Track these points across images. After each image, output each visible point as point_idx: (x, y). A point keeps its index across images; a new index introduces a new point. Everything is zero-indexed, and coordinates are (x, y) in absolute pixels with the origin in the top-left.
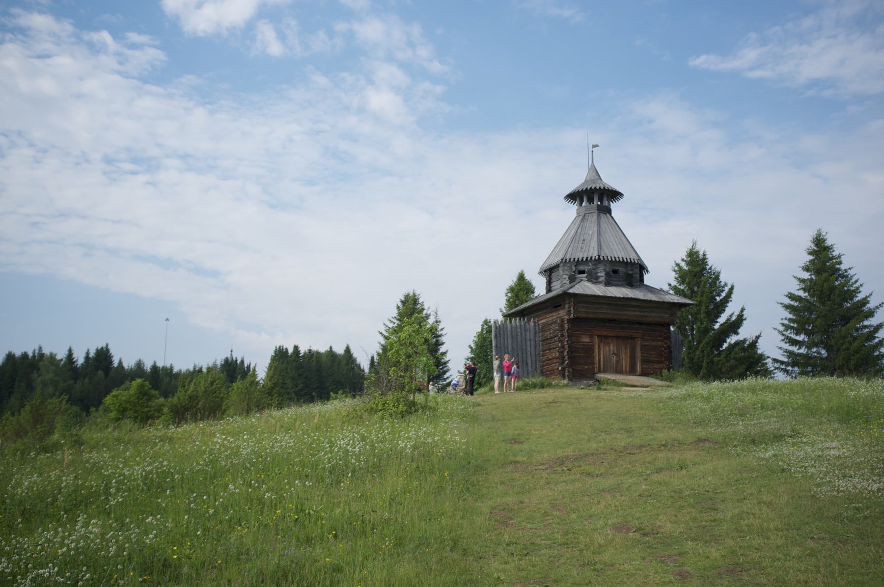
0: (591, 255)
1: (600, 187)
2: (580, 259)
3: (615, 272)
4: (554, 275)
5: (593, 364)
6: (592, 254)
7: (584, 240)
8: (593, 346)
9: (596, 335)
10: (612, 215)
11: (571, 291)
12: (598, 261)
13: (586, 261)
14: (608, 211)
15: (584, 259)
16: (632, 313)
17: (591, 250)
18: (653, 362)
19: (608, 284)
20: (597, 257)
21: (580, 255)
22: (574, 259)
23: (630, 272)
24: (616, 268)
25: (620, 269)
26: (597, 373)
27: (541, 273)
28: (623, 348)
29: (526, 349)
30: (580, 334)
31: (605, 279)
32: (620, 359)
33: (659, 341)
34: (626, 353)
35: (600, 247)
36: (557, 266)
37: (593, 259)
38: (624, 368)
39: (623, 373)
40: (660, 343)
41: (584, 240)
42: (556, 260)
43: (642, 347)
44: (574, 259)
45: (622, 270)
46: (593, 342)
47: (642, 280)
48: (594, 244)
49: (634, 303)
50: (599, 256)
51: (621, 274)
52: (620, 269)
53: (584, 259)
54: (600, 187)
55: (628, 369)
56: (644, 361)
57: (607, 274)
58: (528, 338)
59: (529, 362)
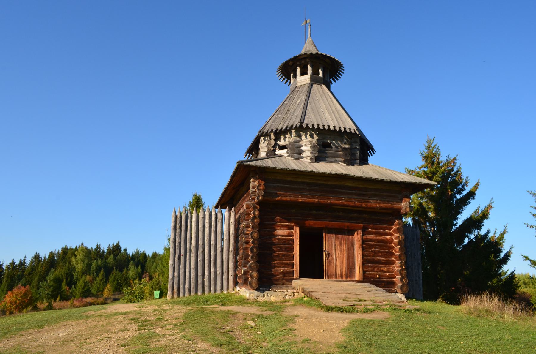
0: (292, 124)
2: (279, 129)
5: (292, 265)
6: (294, 122)
7: (289, 110)
8: (293, 240)
10: (331, 90)
17: (294, 119)
26: (296, 279)
28: (338, 243)
31: (311, 153)
34: (342, 251)
38: (338, 272)
41: (289, 110)
43: (364, 242)
46: (292, 236)
48: (299, 112)
49: (349, 184)
55: (344, 273)
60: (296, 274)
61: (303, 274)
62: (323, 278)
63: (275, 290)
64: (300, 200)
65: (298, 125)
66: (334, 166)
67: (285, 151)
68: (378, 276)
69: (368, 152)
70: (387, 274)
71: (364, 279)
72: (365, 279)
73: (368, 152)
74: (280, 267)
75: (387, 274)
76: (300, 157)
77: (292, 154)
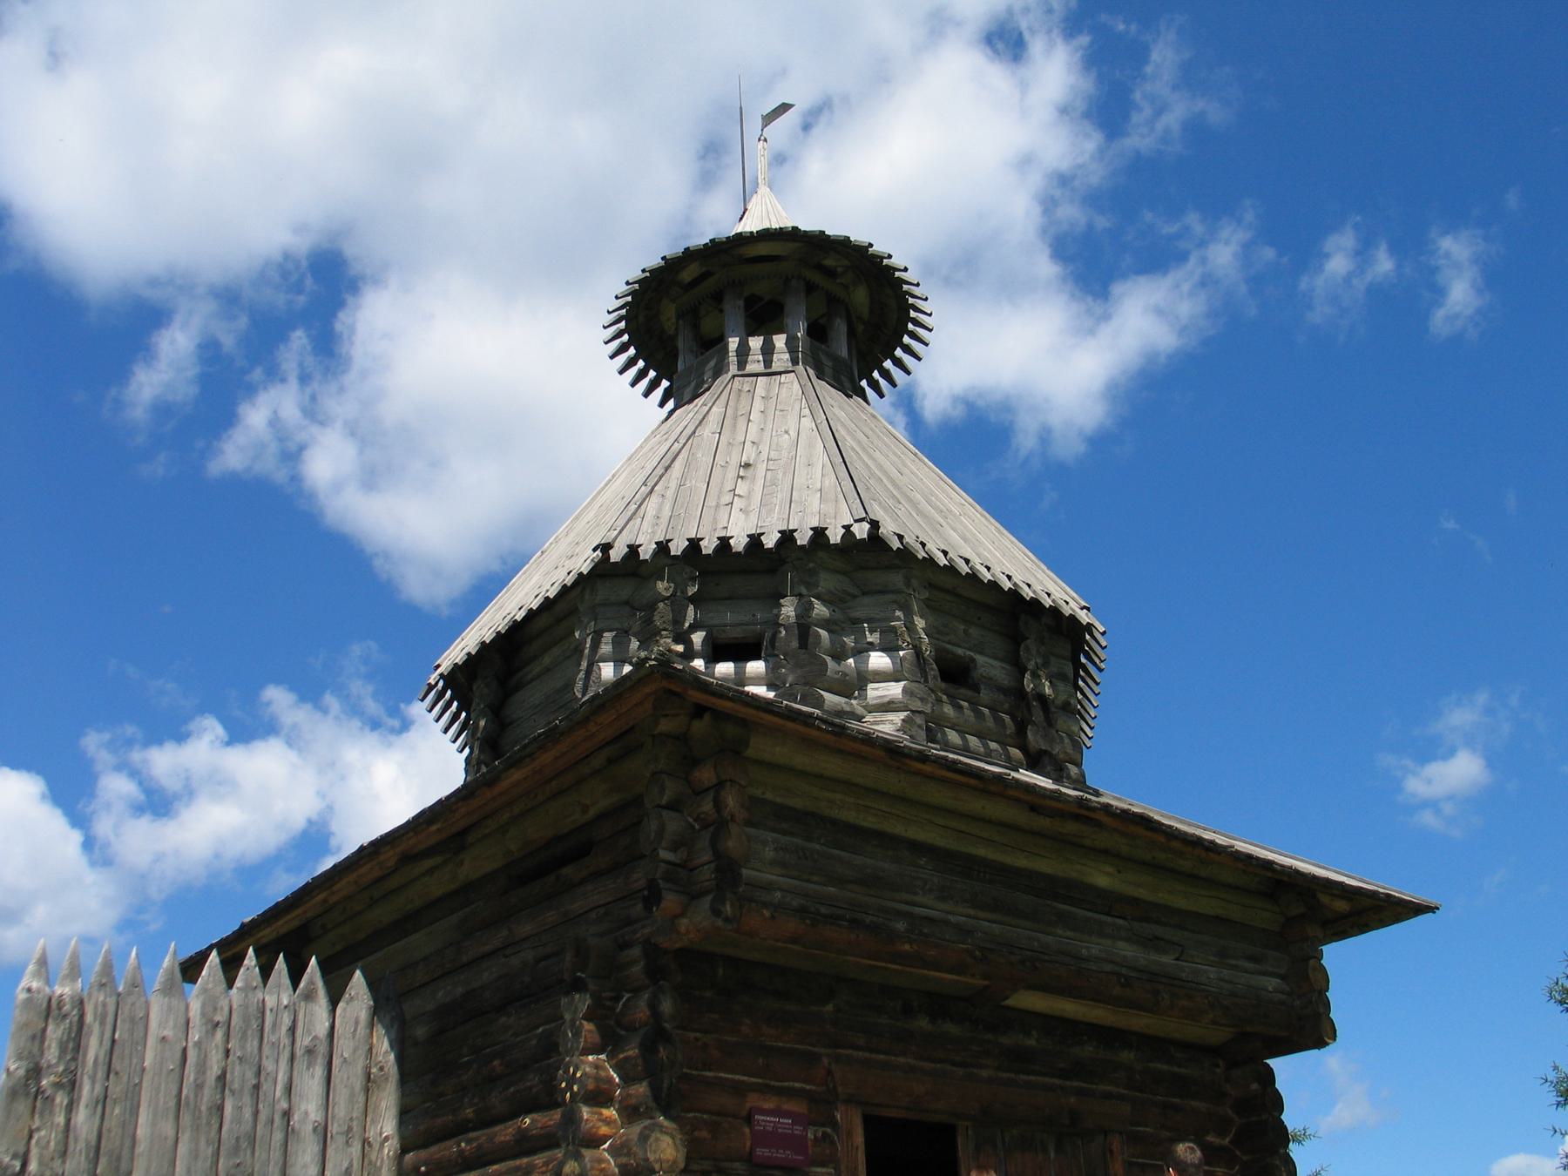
25: (980, 659)
30: (740, 1090)
52: (980, 659)
58: (309, 1108)
65: (861, 531)
77: (806, 684)
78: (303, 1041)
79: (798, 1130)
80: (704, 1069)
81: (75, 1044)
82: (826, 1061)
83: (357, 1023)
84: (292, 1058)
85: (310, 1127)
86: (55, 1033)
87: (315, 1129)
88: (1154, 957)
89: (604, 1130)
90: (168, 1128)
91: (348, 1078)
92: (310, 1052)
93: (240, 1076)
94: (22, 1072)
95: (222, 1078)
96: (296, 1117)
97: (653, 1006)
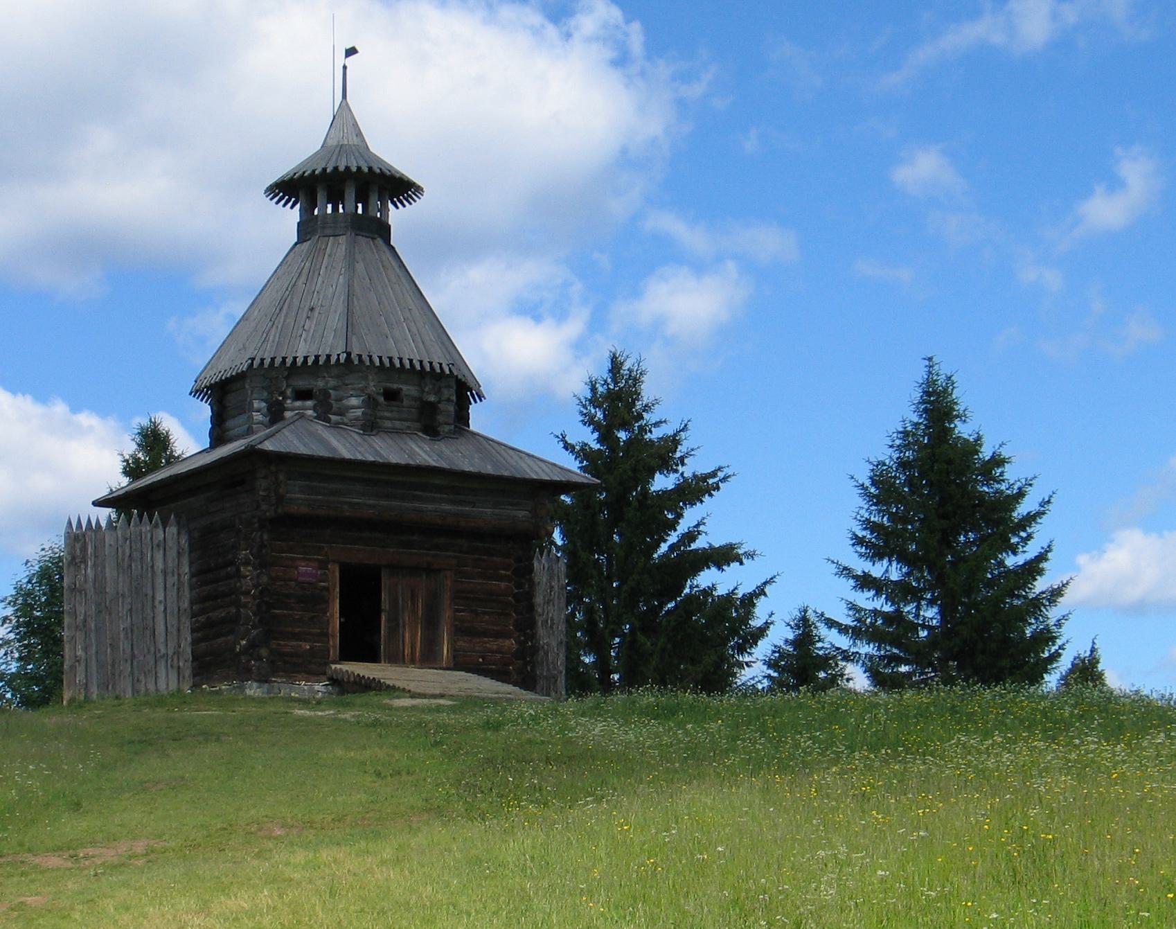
0: (327, 352)
1: (359, 168)
2: (300, 361)
3: (392, 396)
4: (232, 400)
5: (325, 635)
7: (312, 309)
9: (334, 561)
11: (268, 446)
12: (349, 366)
13: (316, 367)
14: (382, 230)
15: (310, 362)
16: (430, 507)
18: (485, 634)
19: (370, 426)
20: (343, 357)
21: (303, 350)
22: (284, 359)
23: (432, 398)
24: (395, 386)
25: (404, 388)
27: (196, 392)
29: (153, 597)
30: (293, 559)
32: (398, 625)
33: (501, 579)
35: (350, 326)
36: (240, 377)
37: (333, 360)
39: (404, 662)
40: (503, 585)
42: (235, 363)
44: (284, 359)
45: (408, 390)
47: (462, 417)
48: (335, 320)
50: (349, 354)
51: (406, 402)
52: (404, 388)
53: (310, 362)
54: (359, 168)
56: (460, 631)
57: (370, 402)
58: (159, 564)
59: (160, 628)
60: (334, 652)
61: (348, 654)
62: (380, 663)
63: (297, 683)
64: (348, 514)
66: (413, 446)
67: (309, 403)
68: (481, 660)
69: (469, 393)
70: (499, 656)
71: (455, 665)
72: (460, 663)
73: (469, 393)
74: (305, 640)
75: (499, 656)
76: (341, 421)
78: (155, 542)
79: (314, 571)
80: (282, 553)
81: (84, 549)
82: (326, 549)
83: (173, 534)
84: (152, 548)
85: (160, 571)
86: (78, 546)
87: (162, 572)
88: (460, 508)
89: (248, 573)
90: (115, 574)
91: (172, 553)
92: (158, 546)
93: (136, 555)
94: (70, 558)
95: (130, 556)
96: (155, 568)
97: (261, 537)
